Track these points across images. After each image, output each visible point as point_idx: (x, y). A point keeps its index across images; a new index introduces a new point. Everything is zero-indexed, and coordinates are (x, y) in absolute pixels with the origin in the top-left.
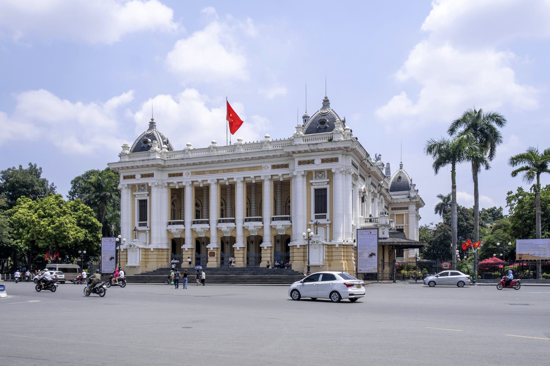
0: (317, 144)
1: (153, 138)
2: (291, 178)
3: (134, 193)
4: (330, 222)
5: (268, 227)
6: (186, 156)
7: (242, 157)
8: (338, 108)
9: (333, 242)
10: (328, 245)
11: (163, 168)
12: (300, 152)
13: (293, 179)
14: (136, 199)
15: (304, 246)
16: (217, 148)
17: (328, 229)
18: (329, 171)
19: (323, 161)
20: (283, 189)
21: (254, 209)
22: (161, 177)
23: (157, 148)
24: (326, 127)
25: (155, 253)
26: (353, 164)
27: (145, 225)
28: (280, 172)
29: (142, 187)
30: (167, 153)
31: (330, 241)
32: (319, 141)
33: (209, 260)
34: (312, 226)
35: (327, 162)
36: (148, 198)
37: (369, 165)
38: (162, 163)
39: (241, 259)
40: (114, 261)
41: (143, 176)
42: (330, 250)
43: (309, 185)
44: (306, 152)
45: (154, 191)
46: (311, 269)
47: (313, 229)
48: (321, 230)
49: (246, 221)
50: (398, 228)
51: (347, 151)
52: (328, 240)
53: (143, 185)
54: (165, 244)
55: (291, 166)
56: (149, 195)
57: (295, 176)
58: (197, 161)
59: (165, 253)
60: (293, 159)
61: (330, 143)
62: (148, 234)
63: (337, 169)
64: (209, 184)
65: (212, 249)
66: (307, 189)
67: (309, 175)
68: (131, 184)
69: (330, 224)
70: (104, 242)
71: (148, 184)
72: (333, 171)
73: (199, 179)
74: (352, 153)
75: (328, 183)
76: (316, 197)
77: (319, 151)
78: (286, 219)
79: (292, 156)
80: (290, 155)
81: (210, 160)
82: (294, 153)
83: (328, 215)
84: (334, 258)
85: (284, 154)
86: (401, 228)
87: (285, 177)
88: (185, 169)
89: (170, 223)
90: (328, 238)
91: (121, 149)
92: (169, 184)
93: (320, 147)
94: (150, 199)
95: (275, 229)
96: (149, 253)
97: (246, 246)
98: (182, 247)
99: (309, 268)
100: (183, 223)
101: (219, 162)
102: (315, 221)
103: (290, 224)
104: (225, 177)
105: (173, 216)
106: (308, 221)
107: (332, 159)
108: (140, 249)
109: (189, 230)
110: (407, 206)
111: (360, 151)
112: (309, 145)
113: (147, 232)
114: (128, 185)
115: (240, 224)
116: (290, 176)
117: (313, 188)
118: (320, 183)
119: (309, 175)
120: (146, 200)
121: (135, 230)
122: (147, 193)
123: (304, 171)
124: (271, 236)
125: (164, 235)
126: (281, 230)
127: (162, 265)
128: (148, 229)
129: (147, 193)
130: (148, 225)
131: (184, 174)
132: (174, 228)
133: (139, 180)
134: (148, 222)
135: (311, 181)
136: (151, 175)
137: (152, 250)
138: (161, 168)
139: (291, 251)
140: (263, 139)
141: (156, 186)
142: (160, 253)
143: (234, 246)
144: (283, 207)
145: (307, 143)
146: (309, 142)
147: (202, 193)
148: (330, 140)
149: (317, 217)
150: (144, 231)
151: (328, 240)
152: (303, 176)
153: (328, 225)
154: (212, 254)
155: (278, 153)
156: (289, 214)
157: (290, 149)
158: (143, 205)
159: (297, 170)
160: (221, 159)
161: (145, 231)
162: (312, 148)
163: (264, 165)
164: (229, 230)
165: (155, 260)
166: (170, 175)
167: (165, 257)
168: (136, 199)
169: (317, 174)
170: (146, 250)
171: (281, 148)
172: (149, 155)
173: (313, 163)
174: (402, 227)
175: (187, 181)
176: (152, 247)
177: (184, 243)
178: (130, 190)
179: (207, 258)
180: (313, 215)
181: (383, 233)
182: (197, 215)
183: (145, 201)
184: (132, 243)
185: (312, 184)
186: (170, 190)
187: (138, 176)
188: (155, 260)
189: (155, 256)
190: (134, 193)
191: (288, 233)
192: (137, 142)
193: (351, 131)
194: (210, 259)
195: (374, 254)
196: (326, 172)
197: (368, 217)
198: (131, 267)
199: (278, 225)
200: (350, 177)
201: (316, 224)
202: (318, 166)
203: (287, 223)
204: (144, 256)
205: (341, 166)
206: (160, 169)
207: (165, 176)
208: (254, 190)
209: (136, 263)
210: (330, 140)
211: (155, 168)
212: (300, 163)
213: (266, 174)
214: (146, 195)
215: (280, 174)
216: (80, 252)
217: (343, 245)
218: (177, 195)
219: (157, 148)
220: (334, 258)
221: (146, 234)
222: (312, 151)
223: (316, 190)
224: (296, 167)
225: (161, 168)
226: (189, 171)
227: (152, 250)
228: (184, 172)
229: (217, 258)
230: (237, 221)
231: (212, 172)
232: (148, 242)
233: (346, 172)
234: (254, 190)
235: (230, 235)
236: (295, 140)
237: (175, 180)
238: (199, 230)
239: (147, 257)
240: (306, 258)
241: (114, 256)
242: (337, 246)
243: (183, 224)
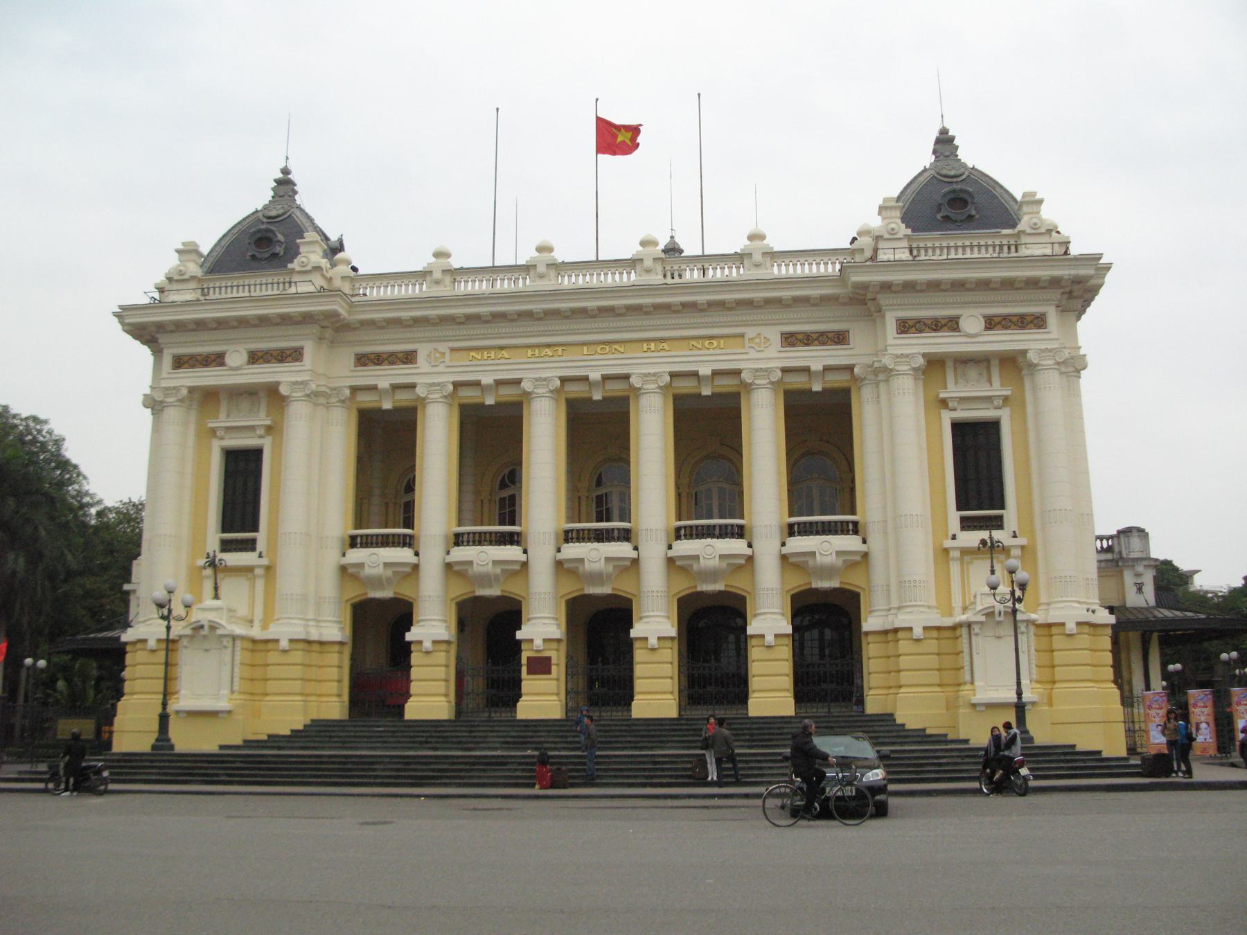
16: (774, 255)
27: (997, 523)
53: (980, 361)
57: (748, 387)
94: (278, 447)
114: (924, 355)
128: (1021, 541)
130: (261, 546)
134: (261, 537)
137: (284, 644)
168: (947, 418)
176: (285, 629)
183: (992, 428)
187: (972, 322)
188: (1087, 672)
189: (297, 671)
211: (1056, 294)
238: (483, 570)
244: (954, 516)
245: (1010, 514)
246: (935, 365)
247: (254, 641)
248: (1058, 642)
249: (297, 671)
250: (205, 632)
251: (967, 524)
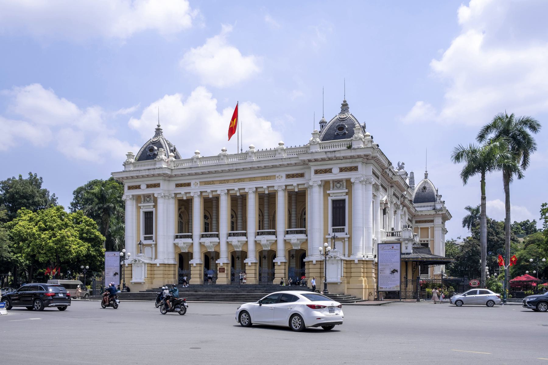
0: (335, 151)
1: (160, 145)
2: (306, 188)
3: (139, 205)
4: (348, 236)
5: (282, 240)
6: (194, 165)
7: (254, 166)
8: (357, 113)
9: (352, 258)
10: (346, 261)
11: (169, 177)
12: (316, 160)
13: (309, 190)
14: (141, 211)
15: (320, 261)
16: (227, 156)
17: (347, 243)
18: (348, 181)
19: (341, 170)
20: (298, 200)
21: (267, 222)
22: (167, 188)
23: (163, 157)
24: (345, 133)
25: (162, 268)
26: (374, 173)
27: (151, 238)
28: (294, 182)
29: (148, 198)
30: (174, 161)
31: (349, 256)
32: (337, 149)
33: (219, 276)
34: (330, 240)
35: (346, 171)
36: (154, 210)
37: (391, 175)
38: (169, 172)
39: (253, 275)
40: (118, 277)
41: (148, 186)
42: (349, 266)
43: (326, 196)
44: (323, 160)
45: (160, 202)
46: (328, 286)
47: (330, 243)
48: (339, 244)
49: (258, 235)
50: (423, 242)
51: (368, 159)
52: (346, 256)
53: (149, 196)
54: (171, 259)
55: (306, 176)
56: (155, 206)
58: (206, 170)
59: (172, 269)
60: (309, 168)
61: (349, 151)
62: (154, 249)
63: (356, 178)
64: (219, 195)
65: (221, 264)
66: (324, 200)
67: (326, 185)
68: (136, 195)
69: (349, 238)
70: (108, 256)
71: (153, 194)
72: (352, 180)
73: (208, 189)
74: (372, 161)
75: (347, 194)
76: (334, 208)
77: (337, 159)
78: (301, 232)
79: (307, 164)
80: (306, 164)
81: (219, 169)
82: (310, 161)
83: (346, 228)
84: (353, 275)
85: (299, 163)
86: (426, 242)
87: (300, 187)
88: (193, 179)
89: (177, 237)
90: (347, 253)
91: (126, 158)
92: (176, 194)
93: (338, 155)
95: (289, 243)
96: (155, 268)
97: (258, 261)
98: (190, 262)
99: (325, 285)
100: (191, 237)
101: (229, 171)
102: (332, 234)
103: (306, 238)
104: (236, 187)
105: (180, 230)
106: (325, 235)
107: (351, 167)
108: (145, 264)
109: (197, 244)
110: (432, 219)
111: (381, 159)
112: (326, 152)
113: (153, 246)
114: (133, 196)
115: (251, 238)
116: (306, 186)
117: (330, 199)
118: (338, 194)
119: (326, 185)
120: (152, 212)
121: (140, 244)
122: (153, 204)
123: (321, 181)
124: (285, 250)
125: (171, 249)
126: (296, 244)
127: (168, 282)
128: (154, 243)
129: (153, 204)
130: (154, 238)
131: (192, 184)
132: (181, 242)
133: (144, 191)
134: (154, 236)
135: (328, 192)
136: (157, 185)
137: (158, 265)
138: (168, 177)
139: (306, 267)
140: (277, 146)
141: (162, 197)
142: (167, 269)
143: (245, 262)
144: (299, 219)
145: (324, 150)
146: (326, 150)
148: (349, 147)
149: (334, 231)
150: (150, 245)
151: (346, 256)
152: (320, 186)
153: (346, 239)
154: (222, 270)
155: (293, 162)
156: (305, 227)
157: (306, 158)
158: (149, 217)
159: (313, 180)
160: (231, 168)
161: (151, 245)
162: (330, 155)
163: (277, 174)
164: (240, 244)
165: (161, 276)
166: (178, 185)
167: (172, 272)
168: (141, 211)
169: (335, 183)
170: (152, 265)
171: (296, 156)
172: (155, 164)
173: (331, 172)
174: (427, 241)
175: (195, 191)
176: (158, 262)
177: (192, 258)
178: (134, 202)
179: (217, 274)
180: (330, 228)
181: (407, 248)
182: (206, 228)
184: (137, 258)
185: (329, 195)
186: (177, 202)
187: (143, 186)
189: (162, 272)
190: (139, 205)
191: (304, 247)
192: (142, 150)
193: (372, 137)
194: (220, 275)
195: (397, 271)
196: (344, 181)
197: (390, 230)
198: (135, 283)
199: (292, 238)
200: (371, 187)
201: (334, 238)
202: (336, 175)
203: (302, 236)
204: (149, 272)
205: (360, 176)
206: (167, 178)
207: (172, 185)
208: (267, 201)
209: (141, 279)
210: (349, 147)
212: (316, 172)
213: (280, 183)
214: (152, 207)
215: (295, 184)
216: (82, 267)
217: (363, 261)
218: (184, 207)
219: (163, 157)
220: (353, 275)
221: (152, 248)
222: (330, 159)
223: (334, 202)
224: (312, 177)
225: (168, 177)
226: (198, 181)
227: (158, 265)
228: (192, 182)
229: (227, 274)
230: (248, 235)
231: (221, 182)
232: (154, 257)
233: (366, 182)
234: (267, 201)
235: (241, 250)
236: (312, 147)
237: (182, 190)
239: (152, 272)
240: (322, 274)
241: (119, 272)
242: (356, 261)
243: (191, 238)
247: (151, 264)
249: (162, 272)
250: (137, 262)
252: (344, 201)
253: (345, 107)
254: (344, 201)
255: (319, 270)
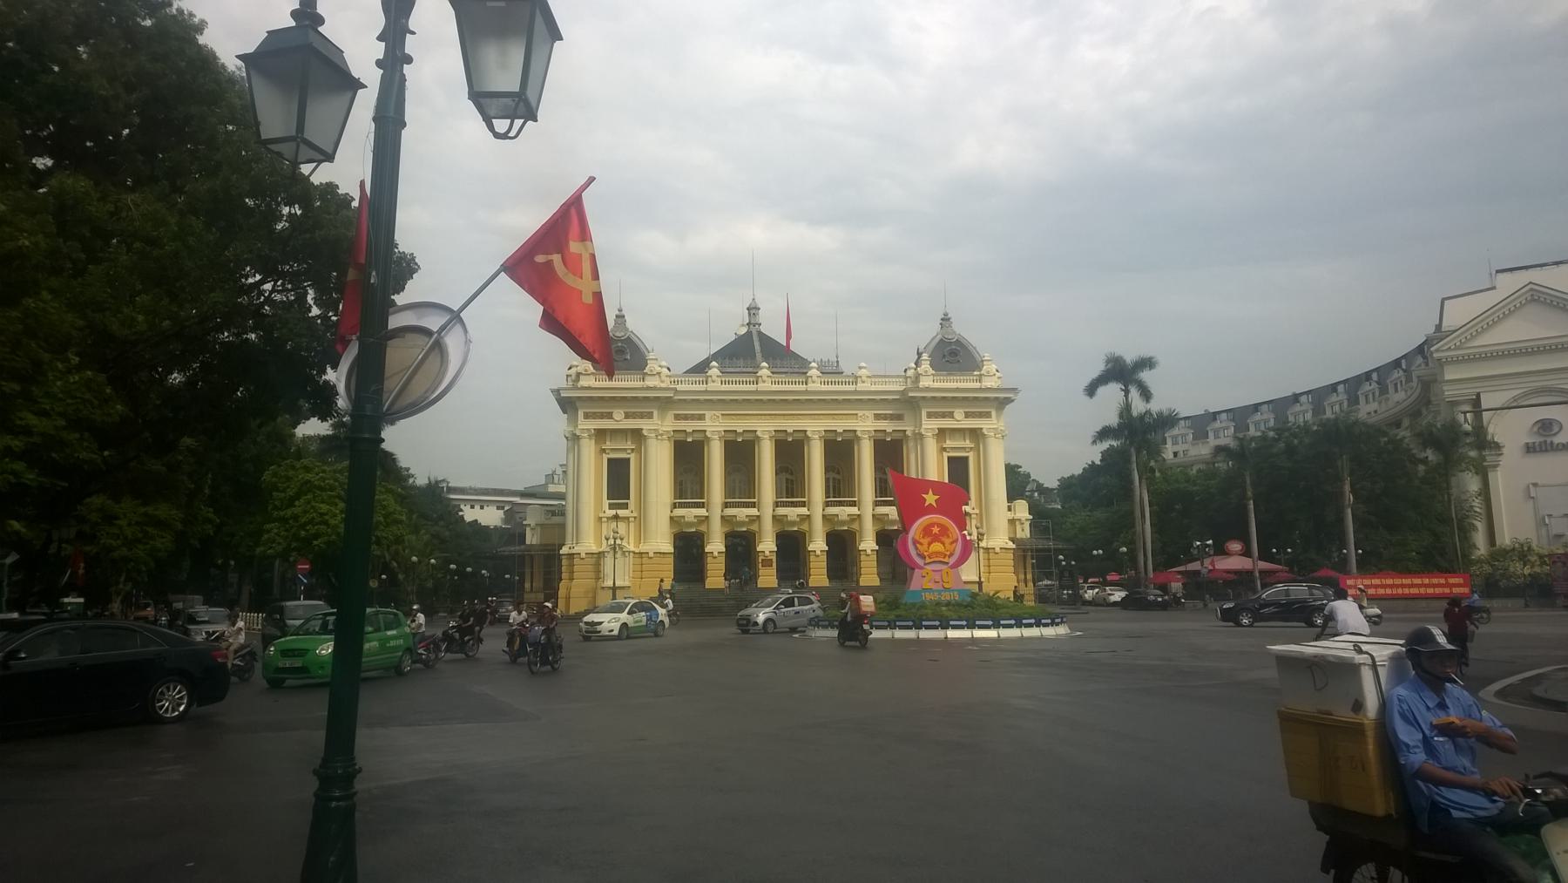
8: (963, 329)
19: (967, 415)
25: (656, 560)
27: (626, 506)
54: (662, 542)
56: (638, 450)
89: (675, 506)
109: (715, 515)
117: (946, 455)
147: (740, 453)
154: (767, 563)
163: (860, 413)
166: (677, 417)
175: (714, 426)
185: (944, 449)
218: (688, 456)
225: (664, 403)
226: (718, 413)
228: (708, 414)
244: (606, 502)
245: (632, 502)
246: (600, 434)
248: (645, 560)
251: (611, 507)
252: (967, 458)
253: (946, 319)
254: (967, 458)
255: (592, 575)
